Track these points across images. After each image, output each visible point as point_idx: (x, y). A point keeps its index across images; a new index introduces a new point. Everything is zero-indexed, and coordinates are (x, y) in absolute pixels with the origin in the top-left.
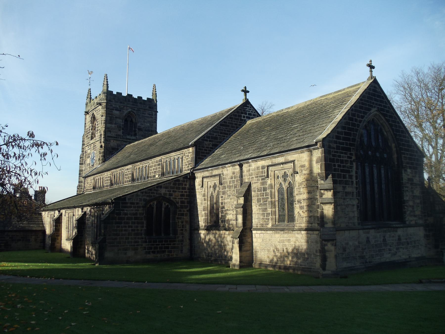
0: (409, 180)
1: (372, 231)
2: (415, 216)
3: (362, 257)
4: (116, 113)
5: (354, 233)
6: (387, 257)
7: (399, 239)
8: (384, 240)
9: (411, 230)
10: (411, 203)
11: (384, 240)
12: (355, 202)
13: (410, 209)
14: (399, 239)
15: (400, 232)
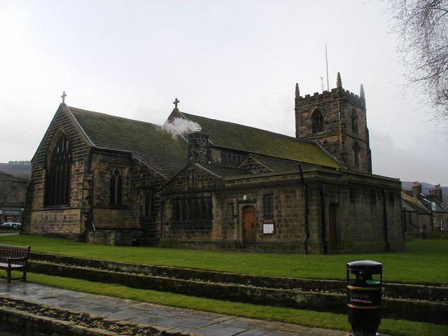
0: (76, 171)
1: (49, 212)
2: (78, 200)
3: (43, 228)
4: (305, 114)
5: (40, 213)
6: (56, 230)
7: (65, 218)
8: (56, 218)
9: (74, 212)
10: (76, 190)
11: (56, 218)
12: (42, 194)
13: (75, 194)
14: (65, 218)
15: (65, 213)
